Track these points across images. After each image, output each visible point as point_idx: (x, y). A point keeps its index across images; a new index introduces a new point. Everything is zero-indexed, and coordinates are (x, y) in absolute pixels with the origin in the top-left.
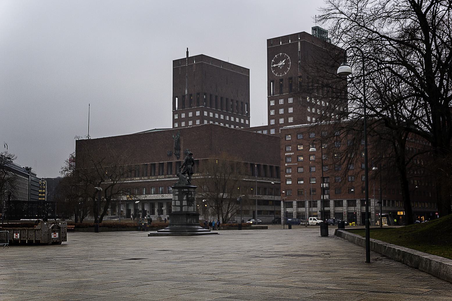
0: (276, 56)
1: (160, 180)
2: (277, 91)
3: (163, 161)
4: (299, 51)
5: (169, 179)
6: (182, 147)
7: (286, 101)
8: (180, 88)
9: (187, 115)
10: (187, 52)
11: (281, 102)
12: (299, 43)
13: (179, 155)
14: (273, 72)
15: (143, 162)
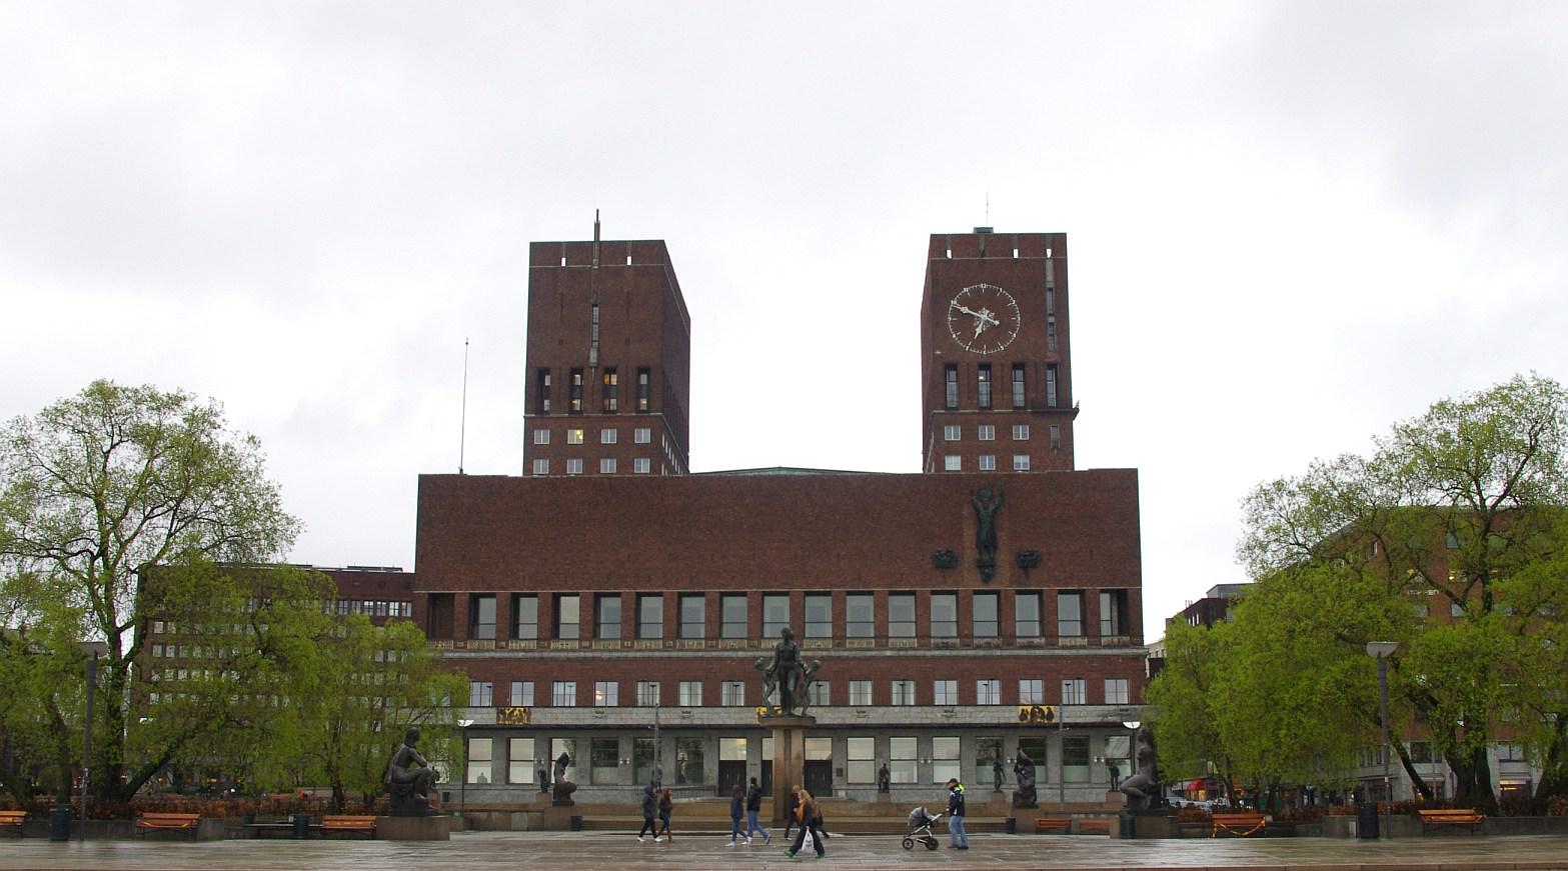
0: (966, 290)
1: (902, 653)
2: (969, 398)
3: (912, 586)
4: (1051, 289)
5: (947, 653)
6: (1003, 538)
7: (1004, 432)
8: (561, 342)
9: (592, 436)
10: (597, 226)
11: (987, 433)
12: (1049, 265)
13: (992, 565)
14: (954, 336)
15: (808, 586)
